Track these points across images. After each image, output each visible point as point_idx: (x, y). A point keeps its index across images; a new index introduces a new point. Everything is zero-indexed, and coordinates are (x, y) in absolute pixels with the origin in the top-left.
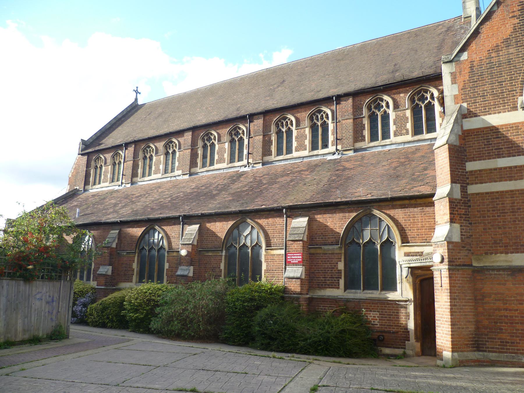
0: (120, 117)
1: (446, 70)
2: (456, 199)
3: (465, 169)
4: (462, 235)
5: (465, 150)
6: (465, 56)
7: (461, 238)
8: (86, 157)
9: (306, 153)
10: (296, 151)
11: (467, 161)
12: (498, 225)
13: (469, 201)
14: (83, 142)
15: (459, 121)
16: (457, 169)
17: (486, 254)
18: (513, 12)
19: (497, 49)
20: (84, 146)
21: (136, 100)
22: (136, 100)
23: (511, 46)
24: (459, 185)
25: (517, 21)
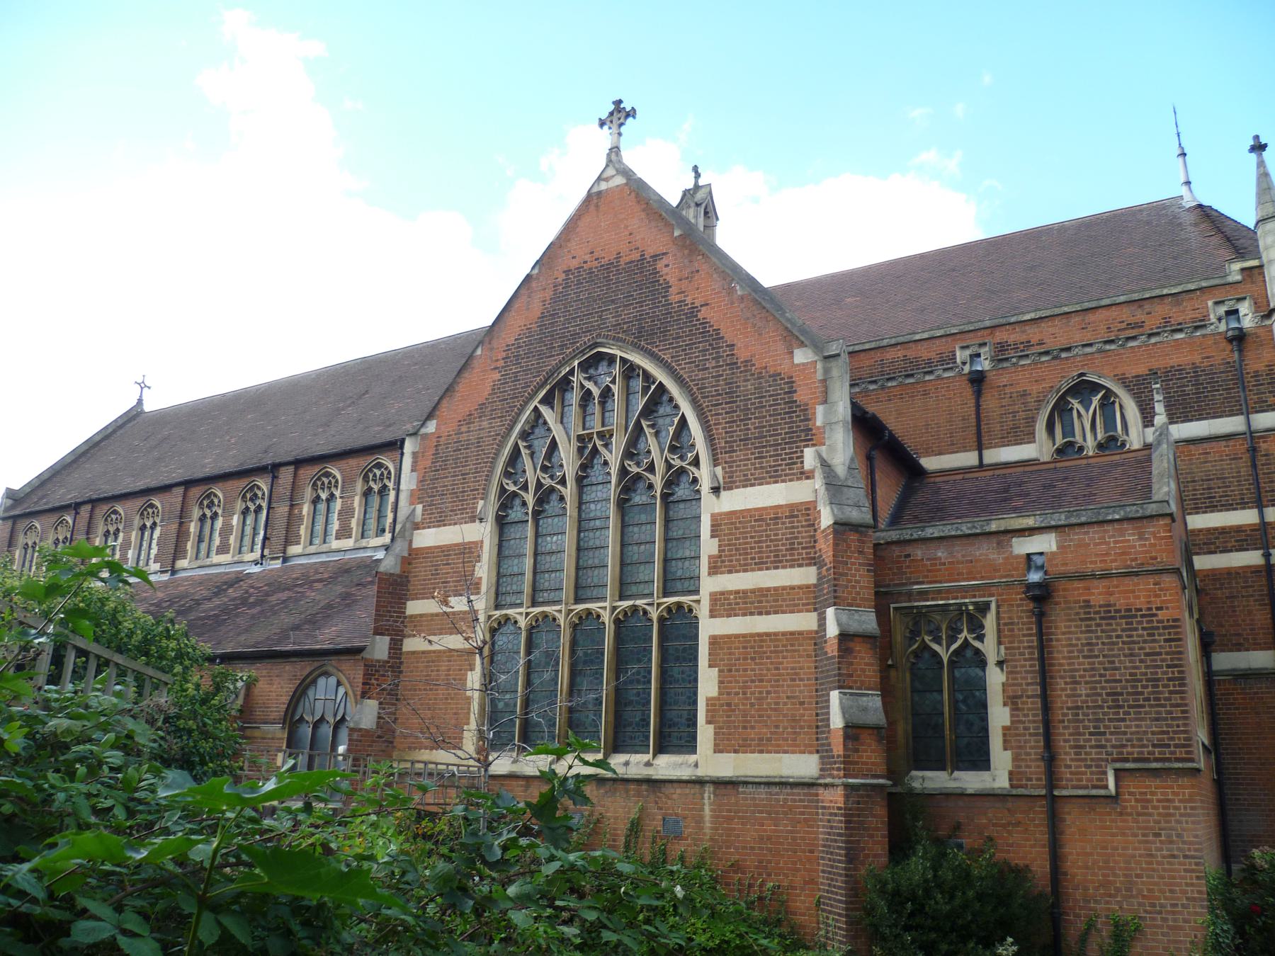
0: (98, 438)
1: (409, 447)
2: (378, 661)
3: (404, 613)
4: (379, 718)
5: (409, 581)
6: (431, 427)
7: (378, 723)
8: (10, 523)
9: (349, 543)
10: (337, 538)
11: (408, 600)
12: (428, 704)
13: (401, 663)
14: (10, 494)
15: (407, 534)
16: (390, 612)
17: (410, 748)
18: (497, 360)
19: (469, 419)
20: (10, 502)
21: (140, 401)
22: (140, 401)
23: (485, 416)
24: (387, 639)
25: (497, 376)
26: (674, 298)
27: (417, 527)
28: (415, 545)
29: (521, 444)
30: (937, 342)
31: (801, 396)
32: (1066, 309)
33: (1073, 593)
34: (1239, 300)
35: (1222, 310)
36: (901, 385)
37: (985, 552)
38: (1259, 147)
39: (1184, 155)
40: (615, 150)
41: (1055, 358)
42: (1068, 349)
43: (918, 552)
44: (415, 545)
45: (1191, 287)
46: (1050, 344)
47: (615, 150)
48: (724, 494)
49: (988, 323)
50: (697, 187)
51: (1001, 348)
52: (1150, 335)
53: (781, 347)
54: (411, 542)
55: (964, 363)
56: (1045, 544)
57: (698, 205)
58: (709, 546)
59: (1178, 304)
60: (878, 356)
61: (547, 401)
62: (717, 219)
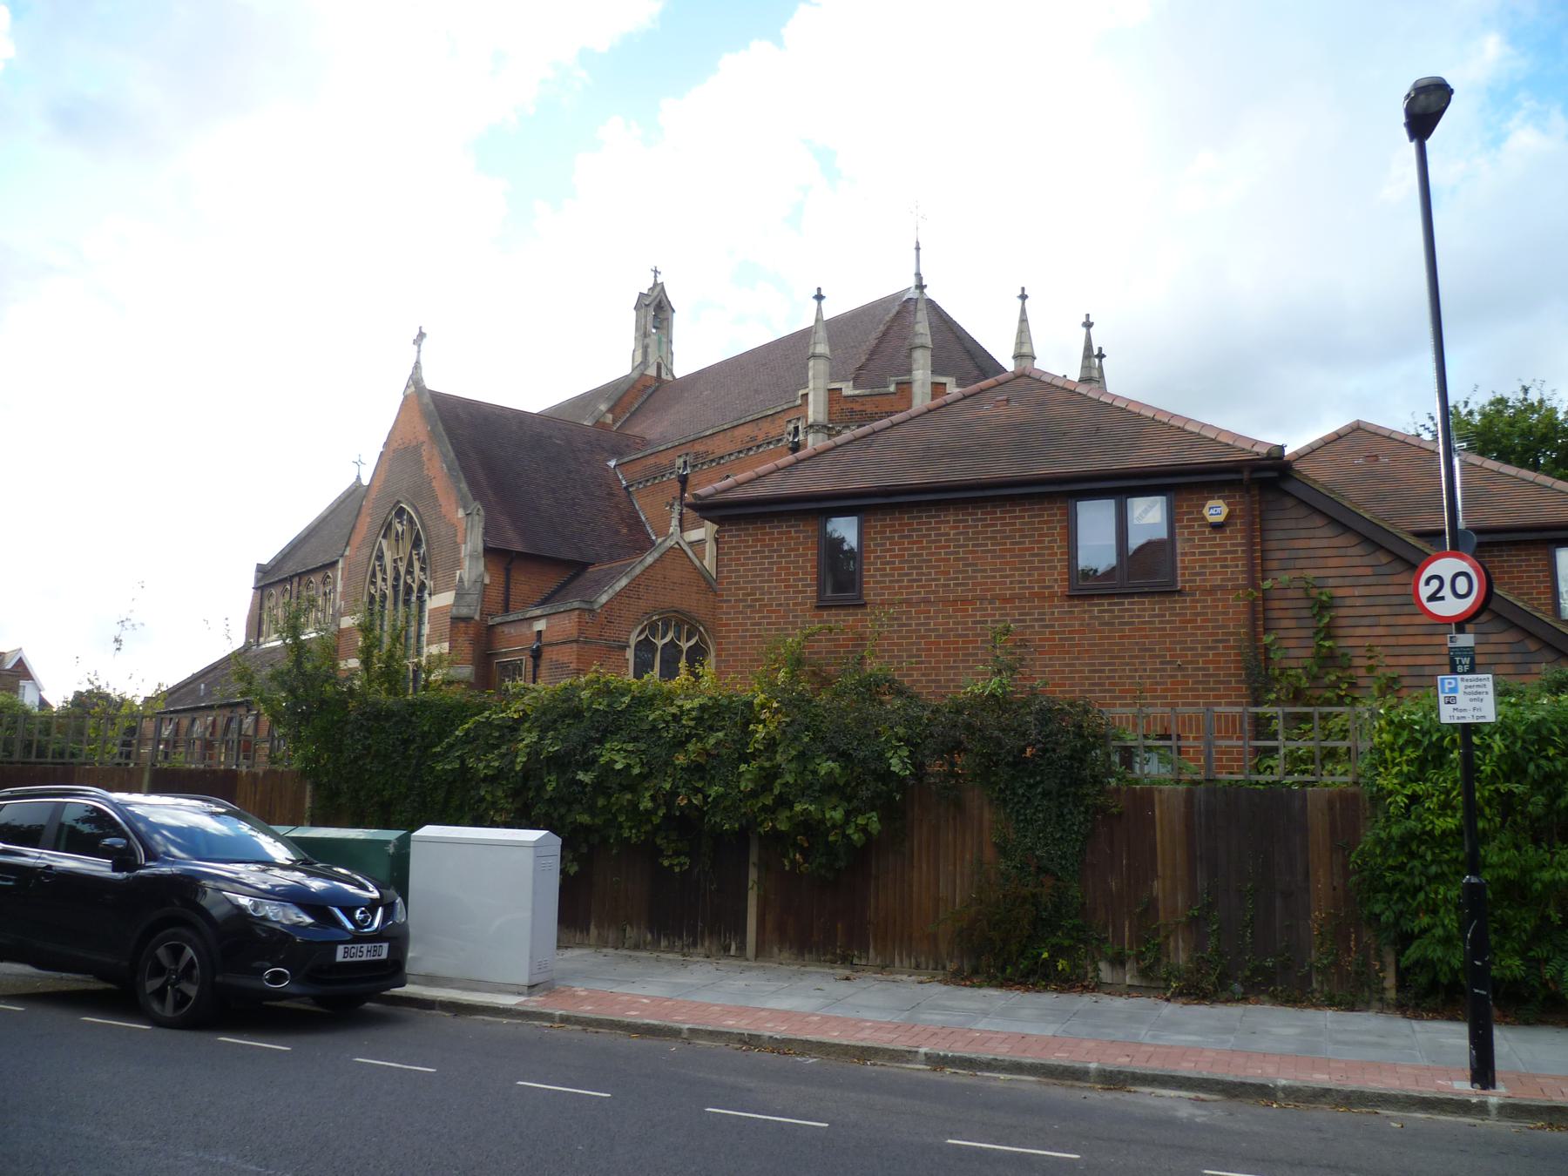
1: (340, 565)
19: (358, 548)
20: (261, 574)
22: (358, 478)
26: (426, 472)
27: (342, 615)
28: (342, 627)
29: (377, 563)
30: (670, 451)
31: (459, 540)
32: (725, 427)
33: (548, 655)
34: (798, 419)
35: (791, 427)
36: (653, 484)
37: (523, 629)
38: (819, 297)
39: (918, 249)
40: (417, 366)
41: (718, 464)
42: (722, 458)
43: (506, 629)
44: (342, 627)
45: (779, 409)
46: (718, 453)
47: (417, 366)
48: (433, 597)
49: (692, 438)
50: (656, 284)
51: (697, 455)
52: (759, 447)
53: (454, 506)
54: (339, 625)
55: (679, 468)
56: (540, 625)
57: (647, 306)
58: (426, 629)
59: (773, 422)
60: (644, 462)
61: (384, 537)
62: (673, 311)
